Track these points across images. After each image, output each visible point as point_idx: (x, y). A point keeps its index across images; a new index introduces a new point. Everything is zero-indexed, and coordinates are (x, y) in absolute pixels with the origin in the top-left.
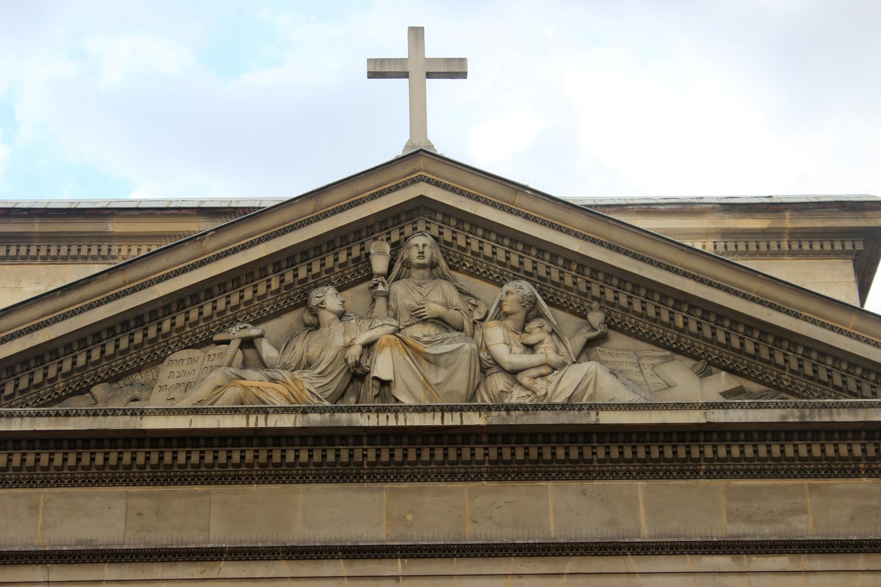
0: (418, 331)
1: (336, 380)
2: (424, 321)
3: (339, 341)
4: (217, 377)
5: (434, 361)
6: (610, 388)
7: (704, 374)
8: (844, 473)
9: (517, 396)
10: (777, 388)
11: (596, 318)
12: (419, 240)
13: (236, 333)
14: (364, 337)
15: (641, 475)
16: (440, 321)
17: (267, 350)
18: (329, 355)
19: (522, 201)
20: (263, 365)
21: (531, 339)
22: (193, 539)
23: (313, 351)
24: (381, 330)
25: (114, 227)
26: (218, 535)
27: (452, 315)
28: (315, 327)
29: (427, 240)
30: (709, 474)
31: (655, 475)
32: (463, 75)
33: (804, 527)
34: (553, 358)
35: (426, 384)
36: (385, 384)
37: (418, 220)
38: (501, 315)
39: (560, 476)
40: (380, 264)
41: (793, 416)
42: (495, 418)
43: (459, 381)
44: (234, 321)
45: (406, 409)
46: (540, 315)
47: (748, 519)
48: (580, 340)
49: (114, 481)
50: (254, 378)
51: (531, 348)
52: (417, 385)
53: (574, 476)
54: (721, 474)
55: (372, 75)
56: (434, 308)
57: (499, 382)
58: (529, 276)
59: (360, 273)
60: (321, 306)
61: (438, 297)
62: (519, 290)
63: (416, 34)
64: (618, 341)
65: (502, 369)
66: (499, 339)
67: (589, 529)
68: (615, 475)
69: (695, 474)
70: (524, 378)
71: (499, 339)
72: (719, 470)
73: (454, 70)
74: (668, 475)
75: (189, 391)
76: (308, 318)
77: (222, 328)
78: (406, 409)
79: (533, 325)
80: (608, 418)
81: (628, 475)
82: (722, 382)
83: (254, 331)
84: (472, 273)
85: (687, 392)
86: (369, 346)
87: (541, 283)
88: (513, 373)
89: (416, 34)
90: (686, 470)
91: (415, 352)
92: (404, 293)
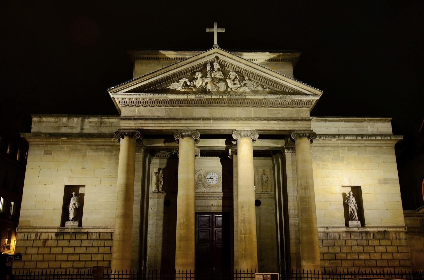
15: (253, 107)
21: (235, 82)
26: (181, 115)
29: (217, 64)
33: (280, 116)
47: (270, 115)
51: (235, 84)
69: (262, 107)
79: (235, 80)
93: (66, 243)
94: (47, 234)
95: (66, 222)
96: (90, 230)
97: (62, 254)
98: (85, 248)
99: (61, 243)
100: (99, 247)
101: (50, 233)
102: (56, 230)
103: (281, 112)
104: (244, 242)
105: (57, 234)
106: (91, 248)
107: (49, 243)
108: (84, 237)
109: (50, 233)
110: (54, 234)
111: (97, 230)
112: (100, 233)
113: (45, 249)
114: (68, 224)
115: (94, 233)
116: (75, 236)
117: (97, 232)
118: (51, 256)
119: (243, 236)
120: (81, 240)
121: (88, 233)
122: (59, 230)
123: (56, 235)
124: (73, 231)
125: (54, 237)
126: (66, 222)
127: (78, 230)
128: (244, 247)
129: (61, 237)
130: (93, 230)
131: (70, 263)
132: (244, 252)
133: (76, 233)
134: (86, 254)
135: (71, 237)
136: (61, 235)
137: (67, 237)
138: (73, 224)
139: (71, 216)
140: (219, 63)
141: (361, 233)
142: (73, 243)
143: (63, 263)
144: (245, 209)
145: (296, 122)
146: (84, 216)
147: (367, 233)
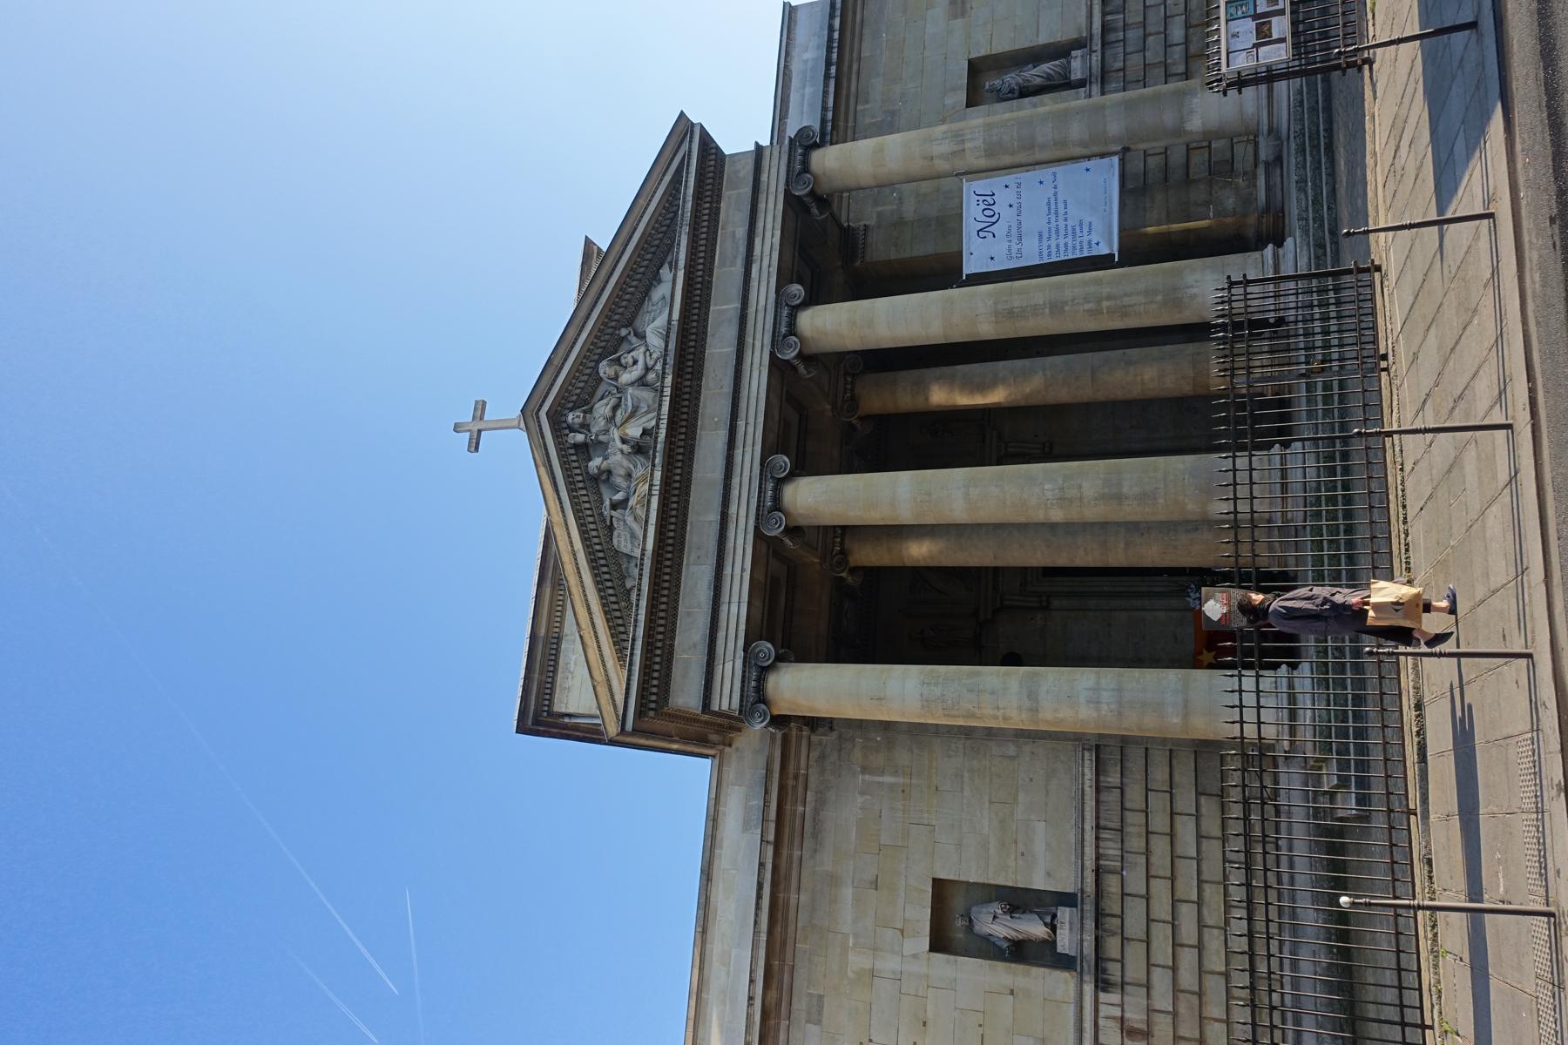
0: (618, 419)
1: (640, 459)
2: (614, 417)
3: (619, 456)
4: (630, 520)
5: (635, 409)
6: (661, 321)
7: (660, 281)
8: (718, 214)
9: (659, 367)
10: (670, 247)
11: (624, 332)
12: (570, 417)
13: (607, 512)
14: (619, 444)
15: (708, 308)
16: (615, 408)
17: (619, 496)
18: (625, 463)
19: (557, 361)
20: (626, 500)
21: (630, 361)
22: (714, 529)
23: (622, 472)
24: (615, 434)
25: (542, 632)
26: (714, 517)
27: (613, 401)
28: (609, 472)
30: (711, 276)
31: (708, 302)
32: (484, 403)
33: (741, 232)
34: (642, 349)
35: (647, 412)
36: (645, 432)
37: (562, 412)
38: (616, 378)
39: (703, 346)
40: (580, 438)
41: (686, 229)
42: (669, 370)
43: (646, 395)
44: (601, 514)
45: (658, 424)
46: (618, 359)
48: (634, 339)
49: (679, 572)
50: (632, 502)
51: (635, 362)
52: (647, 415)
53: (704, 340)
54: (711, 271)
55: (477, 449)
56: (607, 411)
57: (651, 376)
58: (598, 362)
59: (584, 450)
60: (599, 468)
61: (602, 409)
62: (605, 369)
63: (457, 428)
64: (638, 323)
65: (644, 376)
66: (626, 377)
67: (731, 332)
68: (706, 320)
69: (710, 282)
70: (650, 363)
71: (626, 377)
72: (709, 271)
73: (481, 407)
74: (709, 295)
75: (636, 536)
76: (604, 477)
77: (604, 521)
78: (658, 424)
80: (676, 316)
81: (707, 314)
82: (665, 272)
83: (607, 503)
84: (592, 395)
85: (670, 286)
86: (624, 441)
87: (602, 357)
88: (647, 369)
89: (457, 428)
90: (707, 286)
91: (630, 415)
92: (598, 425)
93: (1135, 953)
94: (1101, 1022)
95: (1060, 950)
96: (1090, 864)
97: (1174, 969)
98: (1153, 882)
99: (1135, 971)
100: (1148, 833)
101: (1097, 1010)
102: (1089, 989)
103: (730, 229)
104: (1126, 301)
105: (1102, 984)
106: (1153, 859)
107: (1136, 1017)
108: (1112, 884)
109: (1097, 1010)
110: (1102, 995)
111: (1090, 836)
112: (1098, 827)
113: (1156, 1033)
114: (1065, 942)
115: (1097, 847)
116: (1108, 919)
117: (1097, 838)
118: (1182, 1010)
119: (1105, 304)
120: (1123, 894)
121: (1098, 871)
122: (1086, 978)
123: (1104, 990)
124: (1090, 924)
125: (1115, 998)
126: (1060, 950)
127: (1089, 907)
128: (1142, 299)
129: (1114, 970)
130: (1090, 851)
131: (1206, 937)
132: (1160, 298)
133: (1099, 915)
134: (1173, 879)
135: (1114, 934)
136: (1104, 971)
137: (1112, 946)
138: (1067, 926)
139: (1037, 930)
140: (571, 410)
141: (1105, 44)
142: (1135, 925)
143: (1208, 966)
144: (1017, 304)
145: (763, 187)
146: (1039, 883)
147: (1106, 29)
